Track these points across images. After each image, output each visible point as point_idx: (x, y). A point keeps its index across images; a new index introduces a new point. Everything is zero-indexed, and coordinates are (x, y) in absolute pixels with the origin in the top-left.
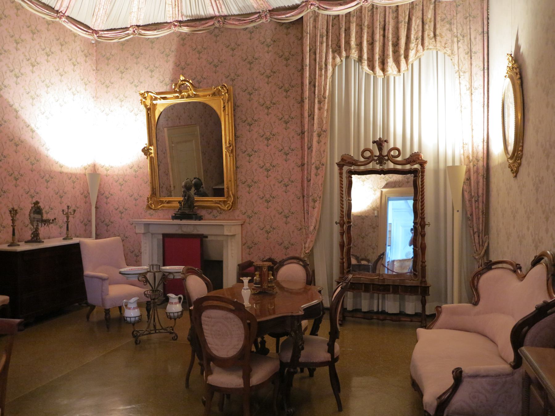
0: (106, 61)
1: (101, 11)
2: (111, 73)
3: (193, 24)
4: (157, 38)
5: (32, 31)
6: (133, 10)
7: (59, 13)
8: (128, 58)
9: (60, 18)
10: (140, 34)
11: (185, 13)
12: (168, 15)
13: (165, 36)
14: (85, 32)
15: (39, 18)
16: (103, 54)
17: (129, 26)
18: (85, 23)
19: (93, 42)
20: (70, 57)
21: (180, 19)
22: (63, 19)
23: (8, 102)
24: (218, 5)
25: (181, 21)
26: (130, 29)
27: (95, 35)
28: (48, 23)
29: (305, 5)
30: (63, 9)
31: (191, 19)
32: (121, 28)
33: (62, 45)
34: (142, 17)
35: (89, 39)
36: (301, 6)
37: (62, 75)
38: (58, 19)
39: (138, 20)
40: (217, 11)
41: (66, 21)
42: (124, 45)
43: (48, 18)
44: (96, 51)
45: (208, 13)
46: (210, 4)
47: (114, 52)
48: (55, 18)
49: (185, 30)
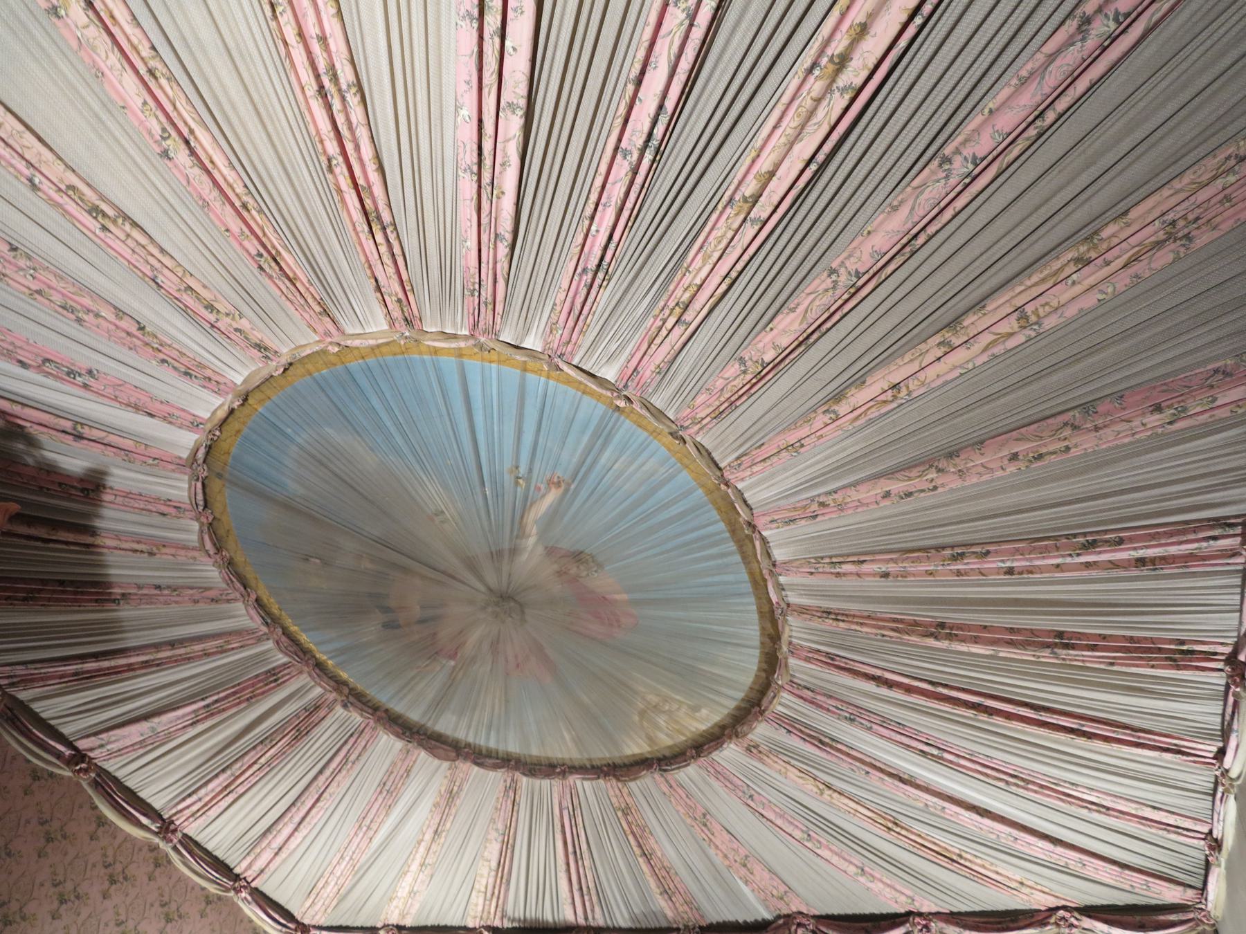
1: (329, 889)
9: (238, 891)
11: (510, 912)
12: (472, 913)
14: (279, 927)
15: (195, 886)
17: (379, 925)
18: (287, 907)
21: (497, 923)
22: (244, 894)
24: (587, 904)
25: (497, 928)
28: (208, 900)
29: (785, 924)
30: (250, 875)
31: (522, 926)
34: (413, 911)
36: (774, 925)
38: (232, 894)
39: (403, 916)
40: (583, 917)
41: (249, 898)
43: (212, 889)
45: (561, 917)
46: (570, 901)
48: (227, 890)
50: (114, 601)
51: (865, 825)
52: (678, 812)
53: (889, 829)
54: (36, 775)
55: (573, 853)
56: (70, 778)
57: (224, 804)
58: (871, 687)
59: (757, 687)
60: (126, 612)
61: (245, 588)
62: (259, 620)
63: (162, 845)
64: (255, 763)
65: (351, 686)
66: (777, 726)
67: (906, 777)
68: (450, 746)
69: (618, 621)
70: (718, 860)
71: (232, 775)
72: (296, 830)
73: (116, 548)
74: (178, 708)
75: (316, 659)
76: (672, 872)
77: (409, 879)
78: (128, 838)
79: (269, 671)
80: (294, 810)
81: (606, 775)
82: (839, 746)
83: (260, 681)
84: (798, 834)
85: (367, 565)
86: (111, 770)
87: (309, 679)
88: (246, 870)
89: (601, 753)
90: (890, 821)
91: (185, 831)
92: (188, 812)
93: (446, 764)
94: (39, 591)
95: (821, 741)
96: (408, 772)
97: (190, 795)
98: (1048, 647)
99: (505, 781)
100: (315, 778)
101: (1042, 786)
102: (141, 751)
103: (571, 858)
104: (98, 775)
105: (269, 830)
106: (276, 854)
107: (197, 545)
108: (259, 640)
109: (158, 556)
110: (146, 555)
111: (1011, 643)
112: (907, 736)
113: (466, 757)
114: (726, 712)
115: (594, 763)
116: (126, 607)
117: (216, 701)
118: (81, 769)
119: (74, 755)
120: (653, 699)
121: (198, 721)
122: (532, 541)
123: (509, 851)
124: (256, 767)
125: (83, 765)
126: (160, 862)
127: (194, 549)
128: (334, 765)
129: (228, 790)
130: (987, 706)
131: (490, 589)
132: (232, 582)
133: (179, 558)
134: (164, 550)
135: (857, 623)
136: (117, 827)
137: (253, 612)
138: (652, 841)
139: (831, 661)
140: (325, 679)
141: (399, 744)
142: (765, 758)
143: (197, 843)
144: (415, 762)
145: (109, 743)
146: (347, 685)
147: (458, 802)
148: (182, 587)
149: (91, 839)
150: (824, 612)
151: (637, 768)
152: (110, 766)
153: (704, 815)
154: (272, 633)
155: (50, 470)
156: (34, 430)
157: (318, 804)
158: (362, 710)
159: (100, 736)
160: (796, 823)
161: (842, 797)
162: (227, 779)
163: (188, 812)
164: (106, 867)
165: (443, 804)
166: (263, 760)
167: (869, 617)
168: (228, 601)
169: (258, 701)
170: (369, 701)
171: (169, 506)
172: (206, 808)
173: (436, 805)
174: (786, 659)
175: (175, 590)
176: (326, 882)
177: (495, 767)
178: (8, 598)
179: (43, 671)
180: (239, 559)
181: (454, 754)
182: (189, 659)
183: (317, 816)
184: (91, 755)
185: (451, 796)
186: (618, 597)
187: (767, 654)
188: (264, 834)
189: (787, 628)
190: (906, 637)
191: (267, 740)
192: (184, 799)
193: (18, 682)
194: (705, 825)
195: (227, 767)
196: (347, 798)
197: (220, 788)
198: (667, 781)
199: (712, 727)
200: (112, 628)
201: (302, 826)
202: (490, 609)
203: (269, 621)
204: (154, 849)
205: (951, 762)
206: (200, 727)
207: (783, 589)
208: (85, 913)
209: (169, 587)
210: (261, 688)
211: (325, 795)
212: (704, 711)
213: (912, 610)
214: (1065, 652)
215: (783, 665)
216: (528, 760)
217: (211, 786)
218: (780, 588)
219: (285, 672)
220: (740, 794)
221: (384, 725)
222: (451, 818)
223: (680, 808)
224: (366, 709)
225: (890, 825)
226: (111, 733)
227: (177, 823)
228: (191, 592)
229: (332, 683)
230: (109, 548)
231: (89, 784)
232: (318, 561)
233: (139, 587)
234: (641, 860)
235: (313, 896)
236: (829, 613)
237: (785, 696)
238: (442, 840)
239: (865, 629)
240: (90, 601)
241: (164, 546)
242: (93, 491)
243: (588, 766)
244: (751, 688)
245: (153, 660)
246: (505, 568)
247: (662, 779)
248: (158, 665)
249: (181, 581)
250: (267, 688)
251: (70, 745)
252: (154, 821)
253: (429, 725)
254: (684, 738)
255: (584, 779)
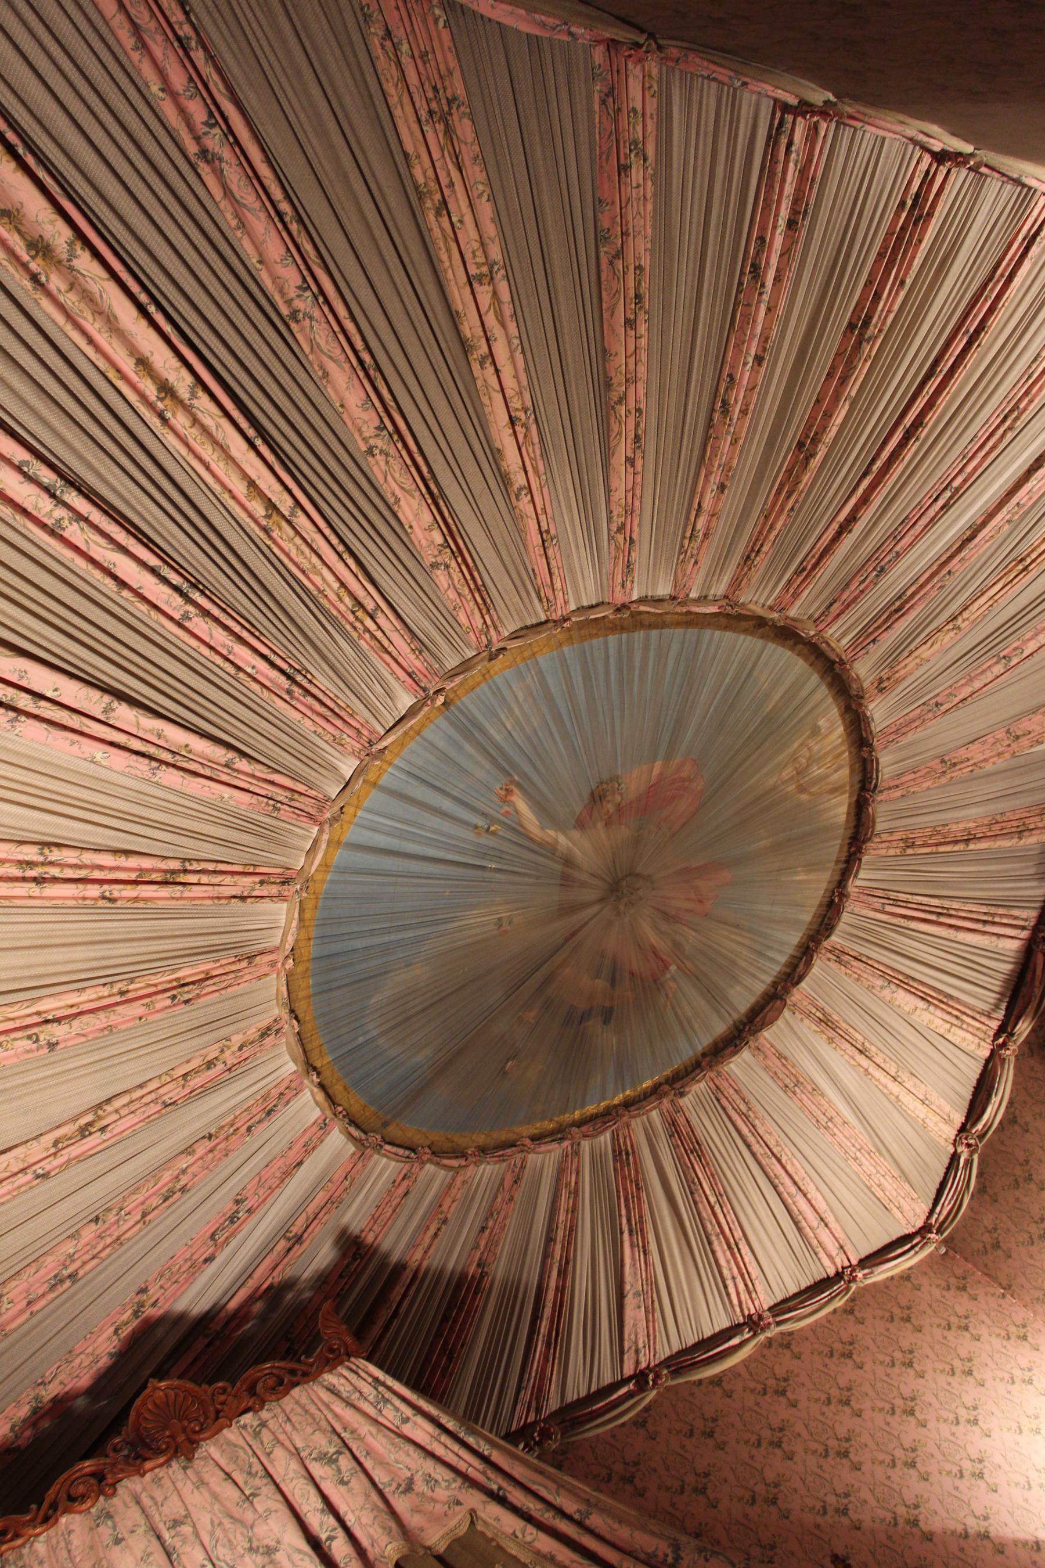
0: (999, 1253)
1: (886, 1184)
2: (1031, 1262)
3: (1020, 1003)
4: (1011, 1103)
5: (843, 1355)
6: (922, 1116)
7: (843, 1272)
8: (1017, 1200)
9: (854, 1279)
10: (981, 1137)
11: (986, 1007)
12: (972, 1047)
13: (1014, 1084)
14: (912, 1252)
16: (981, 1249)
17: (951, 1150)
18: (894, 1238)
19: (943, 1250)
20: (944, 1323)
21: (995, 1025)
22: (860, 1275)
23: (953, 1533)
24: (1005, 921)
25: (1000, 1027)
26: (959, 1150)
27: (929, 1235)
28: (848, 1310)
30: (841, 1261)
31: (1007, 999)
32: (948, 1169)
33: (908, 1319)
34: (947, 1108)
35: (931, 1255)
37: (970, 1373)
39: (948, 1121)
40: (1019, 931)
41: (866, 1271)
42: (985, 1187)
43: (839, 1303)
44: (966, 1259)
46: (994, 939)
47: (988, 1221)
48: (848, 1289)
49: (1024, 1028)
50: (482, 1277)
51: (1011, 594)
52: (928, 789)
53: (1025, 569)
54: (640, 1422)
55: (939, 916)
56: (658, 1393)
57: (748, 1257)
58: (848, 541)
59: (812, 658)
60: (499, 1270)
61: (515, 1146)
62: (554, 1146)
63: (769, 1334)
64: (712, 1208)
65: (663, 1080)
66: (863, 651)
67: (968, 533)
68: (768, 1003)
69: (683, 780)
70: (1001, 763)
71: (717, 1235)
72: (805, 1195)
73: (425, 1252)
74: (622, 1260)
75: (619, 1105)
76: (999, 818)
77: (907, 1099)
78: (745, 1363)
79: (615, 1157)
80: (781, 1188)
81: (859, 850)
82: (909, 593)
83: (622, 1169)
84: (998, 669)
85: (531, 1016)
86: (668, 1353)
87: (638, 1120)
88: (834, 1263)
89: (834, 848)
90: (1016, 565)
91: (766, 1307)
92: (744, 1296)
93: (786, 1013)
94: (446, 1342)
95: (896, 611)
96: (780, 1056)
97: (726, 1287)
98: (860, 343)
99: (829, 960)
100: (753, 1154)
101: (1026, 393)
102: (658, 1314)
103: (942, 919)
104: (668, 1367)
105: (796, 1223)
106: (826, 1225)
107: (451, 1174)
108: (577, 1153)
109: (449, 1216)
110: (444, 1227)
111: (844, 380)
112: (920, 518)
113: (787, 991)
114: (830, 700)
115: (843, 859)
116: (493, 1267)
117: (629, 1221)
118: (653, 1380)
119: (637, 1381)
120: (788, 772)
121: (644, 1247)
122: (562, 839)
123: (911, 983)
124: (717, 1209)
125: (651, 1376)
126: (786, 1342)
127: (454, 1179)
128: (745, 1130)
129: (734, 1246)
130: (912, 425)
131: (601, 900)
132: (502, 1155)
133: (458, 1197)
134: (445, 1207)
135: (769, 532)
136: (730, 1369)
137: (543, 1148)
138: (954, 827)
139: (806, 572)
140: (644, 1103)
141: (746, 1054)
142: (897, 675)
143: (784, 1301)
144: (772, 1046)
145: (636, 1342)
146: (660, 1084)
147: (835, 1017)
148: (491, 1206)
149: (730, 1397)
150: (745, 563)
151: (864, 815)
152: (664, 1352)
153: (943, 761)
154: (572, 1138)
155: (323, 1280)
156: (277, 1277)
157: (783, 1161)
158: (693, 1079)
159: (626, 1349)
160: (985, 666)
161: (971, 608)
162: (720, 1243)
163: (744, 1296)
164: (765, 1393)
165: (831, 1033)
166: (712, 1199)
167: (767, 518)
168: (523, 1167)
169: (644, 1180)
170: (686, 1068)
171: (399, 1184)
172: (746, 1276)
173: (831, 1041)
174: (787, 618)
175: (492, 1214)
176: (879, 1186)
177: (809, 965)
178: (443, 1375)
179: (533, 1374)
180: (481, 1139)
181: (779, 1002)
182: (571, 1228)
183: (797, 1168)
184: (643, 1365)
185: (826, 1022)
186: (656, 771)
187: (776, 634)
188: (800, 1230)
189: (752, 607)
190: (801, 486)
191: (692, 1187)
192: (728, 1295)
193: (538, 1403)
194: (955, 764)
195: (708, 1238)
196: (788, 1130)
197: (728, 1253)
198: (890, 788)
199: (844, 720)
200: (511, 1291)
201: (803, 1188)
202: (622, 908)
203: (559, 1136)
204: (770, 1342)
205: (965, 481)
206: (653, 1247)
207: (706, 597)
208: (799, 1428)
209: (487, 1219)
210: (629, 1171)
211: (775, 1150)
212: (821, 723)
213: (772, 469)
214: (871, 328)
215: (793, 623)
216: (815, 927)
217: (722, 1262)
218: (703, 599)
219: (621, 1141)
220: (930, 715)
221: (718, 1063)
222: (851, 1030)
223: (925, 785)
224: (694, 1074)
225: (1020, 567)
226: (626, 1336)
227: (753, 1311)
228: (499, 1199)
229: (653, 1098)
230: (423, 1259)
231: (672, 1379)
232: (509, 1064)
233: (476, 1247)
234: (972, 847)
235: (891, 1206)
236: (748, 557)
237: (832, 632)
238: (873, 1048)
239: (779, 525)
240: (474, 1299)
241: (440, 1206)
242: (358, 1249)
243: (844, 866)
244: (811, 665)
245: (560, 1265)
246: (584, 877)
247: (885, 793)
248: (567, 1262)
249: (484, 1203)
250: (632, 1165)
251: (625, 1381)
252: (741, 1333)
253: (735, 1016)
254: (847, 754)
255: (856, 876)
